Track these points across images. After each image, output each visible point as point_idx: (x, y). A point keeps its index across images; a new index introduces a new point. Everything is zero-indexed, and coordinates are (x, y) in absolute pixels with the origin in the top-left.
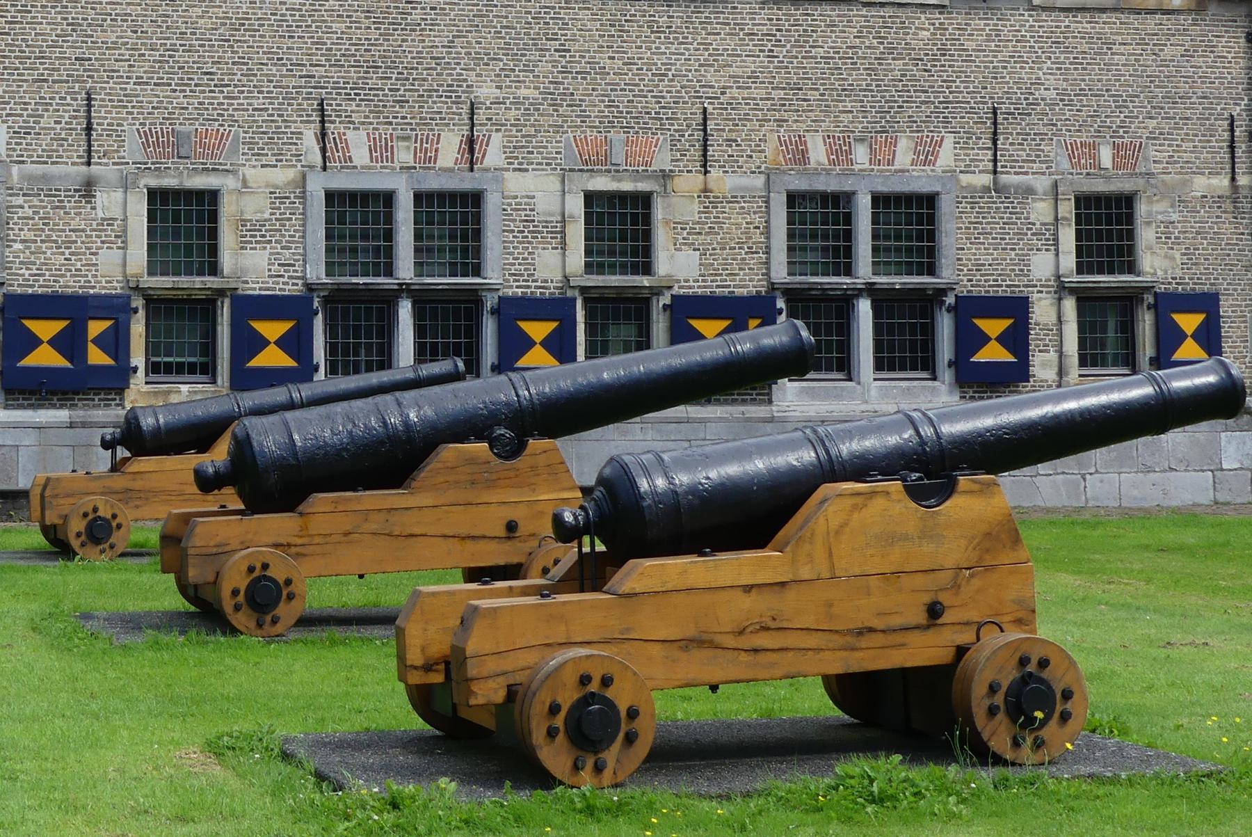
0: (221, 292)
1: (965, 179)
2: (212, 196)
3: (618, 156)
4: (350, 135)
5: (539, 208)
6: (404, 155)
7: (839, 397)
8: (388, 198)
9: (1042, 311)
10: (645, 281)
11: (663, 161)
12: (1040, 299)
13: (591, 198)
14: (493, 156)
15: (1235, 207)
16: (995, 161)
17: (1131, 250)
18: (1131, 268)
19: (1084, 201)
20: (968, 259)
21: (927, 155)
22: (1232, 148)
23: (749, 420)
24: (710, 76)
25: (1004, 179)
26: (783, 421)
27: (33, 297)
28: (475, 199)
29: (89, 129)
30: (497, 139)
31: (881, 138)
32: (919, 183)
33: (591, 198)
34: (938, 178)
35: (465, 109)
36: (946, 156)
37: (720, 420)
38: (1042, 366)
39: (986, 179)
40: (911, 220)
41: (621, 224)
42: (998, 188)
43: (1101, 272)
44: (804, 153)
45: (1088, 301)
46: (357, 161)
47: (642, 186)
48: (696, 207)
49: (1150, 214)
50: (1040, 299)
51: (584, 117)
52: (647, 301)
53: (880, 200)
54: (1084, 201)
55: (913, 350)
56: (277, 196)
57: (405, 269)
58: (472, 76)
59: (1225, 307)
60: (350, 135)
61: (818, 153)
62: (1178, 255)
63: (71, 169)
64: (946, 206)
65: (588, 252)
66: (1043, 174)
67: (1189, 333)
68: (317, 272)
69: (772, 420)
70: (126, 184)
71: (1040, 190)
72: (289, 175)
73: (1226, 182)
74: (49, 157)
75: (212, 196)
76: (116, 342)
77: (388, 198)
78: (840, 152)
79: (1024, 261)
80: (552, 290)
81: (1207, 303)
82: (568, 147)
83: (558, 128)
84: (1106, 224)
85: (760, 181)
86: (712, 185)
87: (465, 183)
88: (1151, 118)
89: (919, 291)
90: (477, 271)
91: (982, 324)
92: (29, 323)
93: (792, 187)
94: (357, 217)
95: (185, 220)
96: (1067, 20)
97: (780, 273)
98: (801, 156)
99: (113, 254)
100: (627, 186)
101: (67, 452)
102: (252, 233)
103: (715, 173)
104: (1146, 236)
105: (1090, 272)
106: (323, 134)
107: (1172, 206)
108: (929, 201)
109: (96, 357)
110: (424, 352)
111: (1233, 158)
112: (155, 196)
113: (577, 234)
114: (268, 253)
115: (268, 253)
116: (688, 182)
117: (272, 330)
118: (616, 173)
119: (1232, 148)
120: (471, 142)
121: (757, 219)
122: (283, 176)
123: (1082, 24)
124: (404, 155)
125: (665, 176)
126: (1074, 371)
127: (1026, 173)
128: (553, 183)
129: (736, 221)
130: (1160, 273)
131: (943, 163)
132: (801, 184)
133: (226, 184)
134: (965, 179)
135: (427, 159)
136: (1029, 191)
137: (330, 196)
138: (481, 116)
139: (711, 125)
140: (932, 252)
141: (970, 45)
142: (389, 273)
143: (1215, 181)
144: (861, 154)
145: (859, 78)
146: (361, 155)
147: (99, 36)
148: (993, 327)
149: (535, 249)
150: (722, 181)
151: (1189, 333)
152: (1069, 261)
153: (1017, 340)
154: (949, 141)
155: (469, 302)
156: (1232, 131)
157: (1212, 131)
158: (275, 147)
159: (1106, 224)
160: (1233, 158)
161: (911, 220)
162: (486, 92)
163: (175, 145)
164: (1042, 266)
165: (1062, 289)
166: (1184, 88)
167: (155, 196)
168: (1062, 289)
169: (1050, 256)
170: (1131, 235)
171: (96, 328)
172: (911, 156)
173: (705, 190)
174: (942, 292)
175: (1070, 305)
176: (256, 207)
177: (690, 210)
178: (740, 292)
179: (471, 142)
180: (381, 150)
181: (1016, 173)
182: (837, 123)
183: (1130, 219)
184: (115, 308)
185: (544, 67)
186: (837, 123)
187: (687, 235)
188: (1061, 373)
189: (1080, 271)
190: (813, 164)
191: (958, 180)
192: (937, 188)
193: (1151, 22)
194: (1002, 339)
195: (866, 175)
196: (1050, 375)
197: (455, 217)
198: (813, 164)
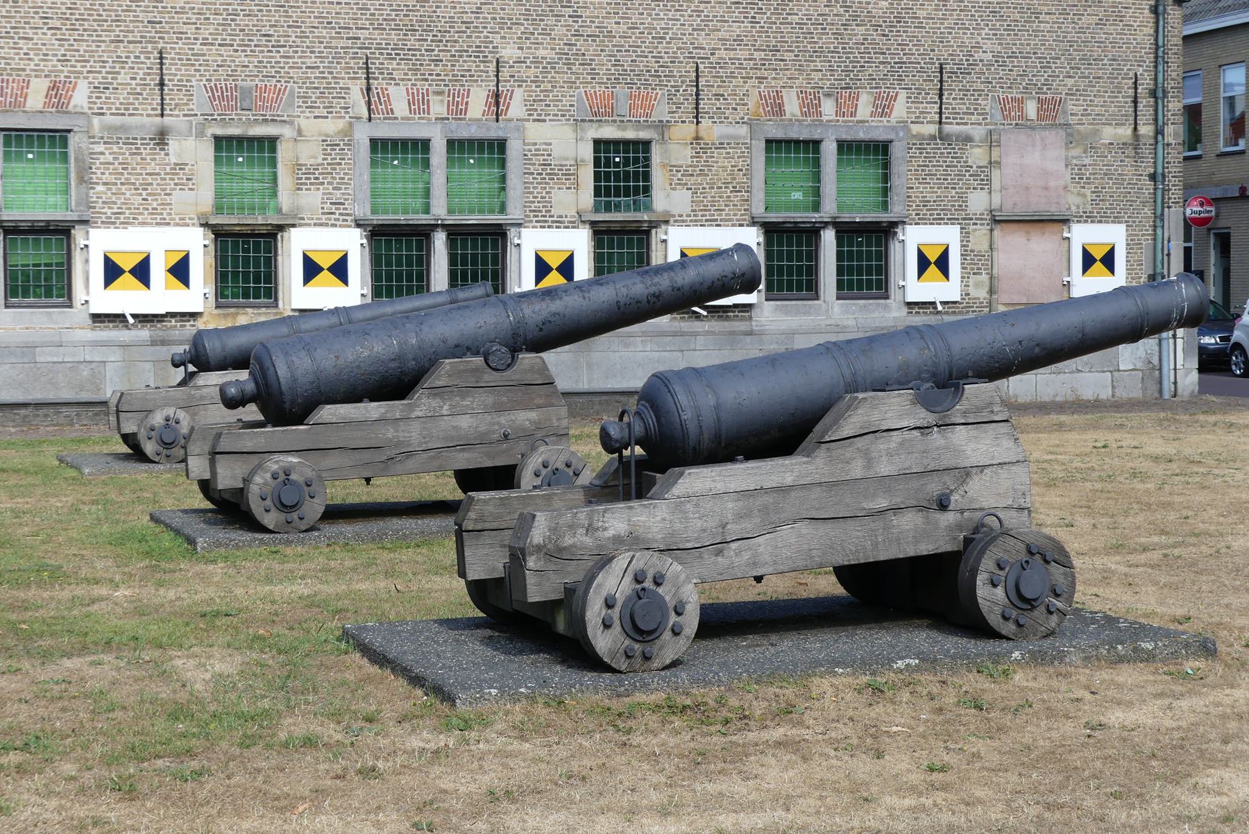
1: (915, 129)
4: (392, 90)
6: (438, 108)
11: (661, 112)
14: (516, 108)
16: (941, 113)
21: (883, 108)
22: (1135, 102)
24: (702, 39)
25: (947, 128)
26: (761, 333)
28: (500, 146)
30: (519, 94)
31: (846, 93)
33: (597, 143)
34: (893, 128)
35: (492, 67)
36: (900, 109)
37: (708, 333)
39: (932, 129)
42: (942, 136)
44: (781, 106)
47: (643, 135)
48: (689, 152)
51: (594, 74)
52: (648, 233)
53: (845, 147)
56: (329, 144)
58: (497, 39)
60: (392, 90)
61: (792, 106)
64: (897, 151)
65: (597, 192)
66: (980, 124)
69: (750, 333)
70: (201, 134)
71: (977, 138)
72: (341, 124)
78: (811, 106)
79: (962, 198)
82: (580, 100)
86: (701, 134)
90: (503, 209)
93: (770, 136)
98: (779, 109)
100: (630, 134)
103: (705, 123)
106: (369, 89)
110: (456, 278)
113: (587, 175)
118: (622, 125)
119: (1135, 102)
120: (497, 95)
122: (332, 126)
124: (438, 108)
125: (662, 127)
127: (966, 124)
132: (780, 135)
133: (287, 132)
134: (915, 129)
135: (458, 110)
136: (968, 139)
137: (374, 142)
138: (505, 73)
139: (702, 82)
142: (427, 211)
144: (828, 108)
145: (828, 42)
146: (400, 108)
150: (712, 130)
154: (903, 95)
156: (1136, 88)
157: (1119, 88)
158: (325, 99)
162: (509, 52)
163: (245, 99)
166: (1097, 52)
172: (871, 109)
173: (697, 138)
176: (310, 153)
177: (683, 155)
179: (497, 95)
180: (418, 104)
181: (958, 124)
185: (559, 31)
190: (788, 116)
191: (909, 130)
195: (830, 123)
198: (788, 116)
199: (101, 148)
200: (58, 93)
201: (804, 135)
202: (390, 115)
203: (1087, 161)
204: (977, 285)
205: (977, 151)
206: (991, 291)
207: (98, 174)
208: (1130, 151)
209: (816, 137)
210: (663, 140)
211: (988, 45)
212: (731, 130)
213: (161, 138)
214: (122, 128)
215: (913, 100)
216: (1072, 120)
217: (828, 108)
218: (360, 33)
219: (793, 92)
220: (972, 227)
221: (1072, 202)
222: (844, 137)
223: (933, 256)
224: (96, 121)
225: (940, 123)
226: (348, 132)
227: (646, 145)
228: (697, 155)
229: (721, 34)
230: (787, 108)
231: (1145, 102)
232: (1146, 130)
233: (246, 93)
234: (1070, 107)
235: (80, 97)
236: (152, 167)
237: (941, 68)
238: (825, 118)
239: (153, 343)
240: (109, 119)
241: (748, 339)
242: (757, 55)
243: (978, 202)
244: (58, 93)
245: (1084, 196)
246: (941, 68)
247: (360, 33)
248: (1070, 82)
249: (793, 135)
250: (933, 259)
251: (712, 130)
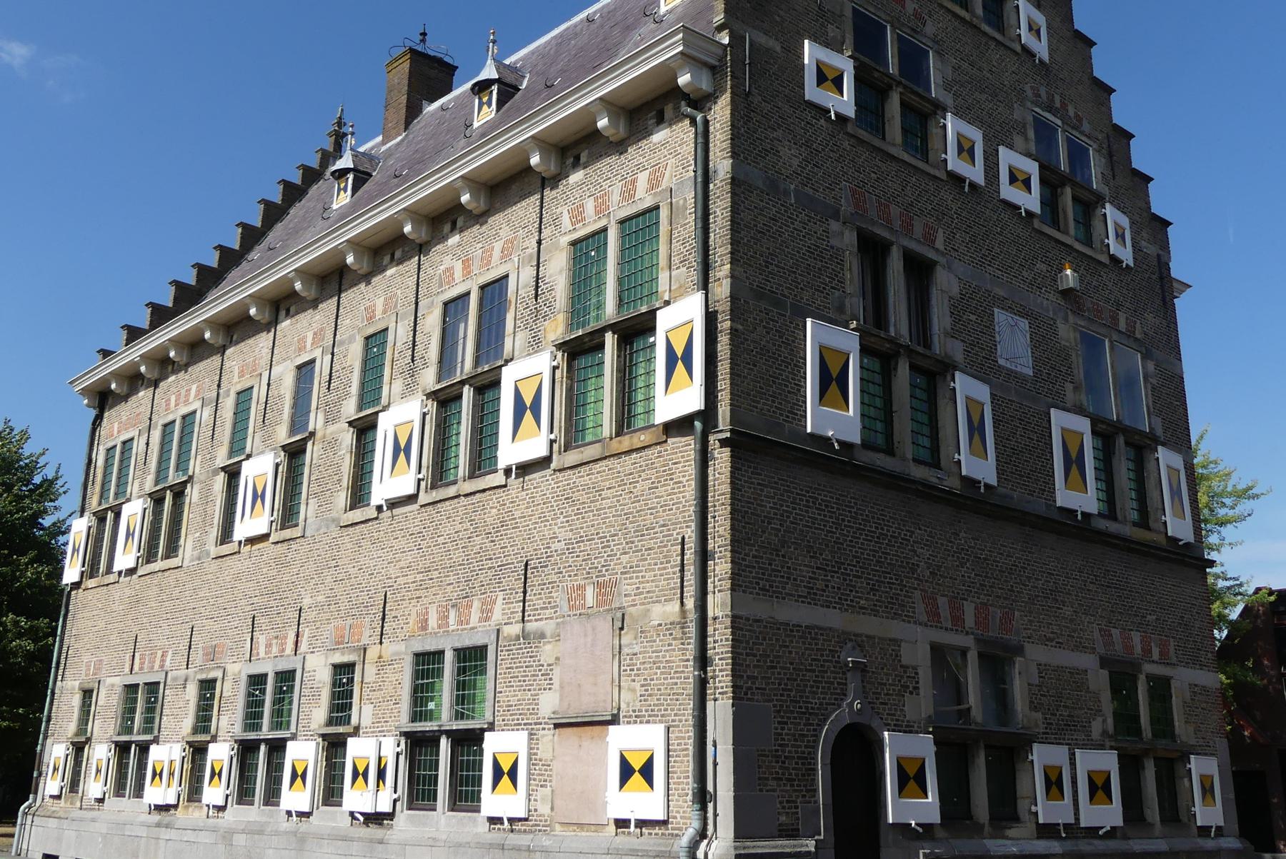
12: (543, 736)
15: (684, 633)
22: (682, 571)
25: (532, 626)
39: (515, 629)
50: (543, 736)
67: (637, 774)
71: (548, 634)
88: (625, 553)
119: (682, 571)
136: (542, 636)
141: (517, 514)
145: (458, 556)
151: (637, 774)
206: (552, 809)
209: (440, 647)
211: (562, 534)
216: (625, 602)
220: (541, 732)
221: (628, 700)
222: (459, 645)
223: (637, 764)
225: (523, 621)
229: (402, 564)
230: (430, 622)
234: (626, 588)
237: (526, 565)
238: (451, 628)
243: (549, 704)
246: (526, 565)
248: (625, 558)
250: (637, 766)
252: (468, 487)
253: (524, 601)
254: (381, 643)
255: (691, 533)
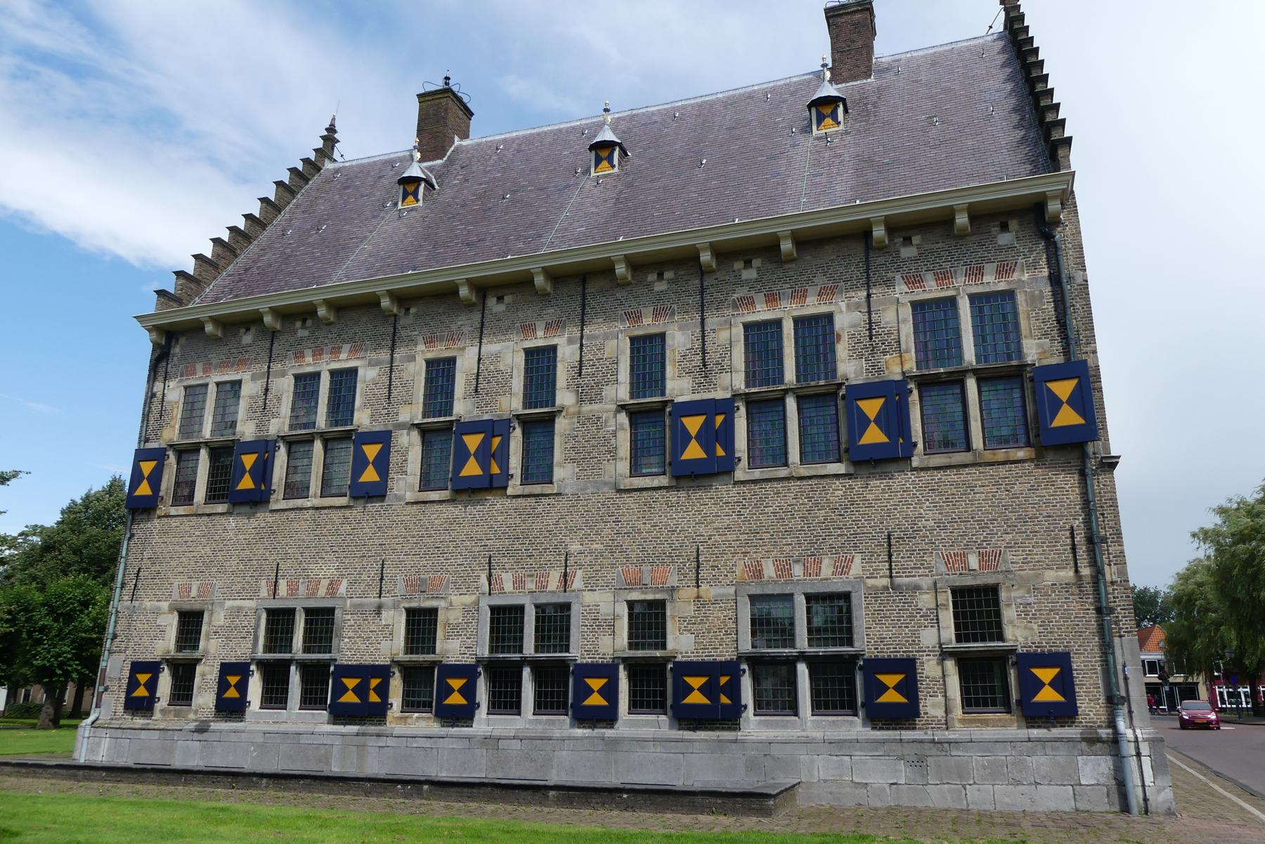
0: (434, 663)
1: (870, 582)
2: (433, 612)
3: (647, 580)
5: (602, 611)
7: (785, 727)
8: (520, 609)
9: (929, 668)
10: (658, 653)
11: (673, 581)
13: (631, 604)
14: (577, 583)
16: (890, 569)
17: (999, 625)
18: (1001, 637)
19: (958, 592)
20: (871, 636)
21: (843, 568)
23: (721, 741)
25: (898, 581)
26: (743, 742)
27: (351, 666)
28: (566, 607)
29: (382, 579)
30: (580, 573)
31: (811, 559)
32: (838, 585)
34: (849, 583)
36: (856, 568)
38: (931, 707)
40: (835, 610)
41: (648, 620)
43: (975, 640)
45: (966, 664)
46: (506, 590)
47: (659, 596)
48: (692, 608)
49: (1009, 598)
51: (628, 559)
54: (958, 592)
55: (842, 695)
56: (466, 610)
57: (529, 648)
59: (1077, 663)
61: (769, 570)
62: (1035, 627)
63: (372, 600)
65: (630, 637)
68: (485, 652)
70: (395, 607)
71: (925, 586)
72: (473, 598)
73: (1071, 573)
74: (364, 595)
75: (433, 612)
76: (383, 690)
77: (520, 609)
78: (784, 570)
80: (608, 660)
81: (1061, 660)
82: (619, 576)
83: (613, 565)
84: (977, 607)
85: (732, 590)
86: (702, 594)
87: (561, 599)
89: (838, 658)
91: (689, 680)
92: (880, 677)
94: (505, 620)
95: (422, 625)
96: (939, 475)
97: (746, 646)
98: (759, 573)
99: (386, 642)
100: (650, 597)
101: (354, 748)
102: (454, 630)
103: (704, 587)
104: (1009, 614)
105: (967, 641)
106: (490, 575)
107: (1028, 592)
108: (846, 596)
109: (374, 698)
111: (1075, 556)
112: (410, 612)
114: (461, 643)
115: (461, 643)
116: (689, 593)
117: (456, 683)
118: (644, 588)
121: (731, 614)
123: (952, 476)
124: (531, 586)
125: (673, 590)
126: (958, 712)
128: (609, 597)
129: (717, 615)
130: (1021, 639)
131: (858, 573)
132: (758, 591)
133: (441, 604)
134: (870, 582)
135: (543, 587)
136: (917, 588)
138: (571, 561)
139: (702, 559)
140: (850, 630)
143: (1062, 573)
144: (798, 570)
145: (796, 523)
146: (508, 586)
147: (390, 532)
148: (891, 680)
149: (600, 636)
150: (708, 591)
152: (949, 633)
153: (910, 687)
154: (858, 558)
155: (562, 666)
156: (1073, 537)
158: (465, 584)
159: (977, 607)
160: (1075, 556)
161: (835, 610)
162: (575, 547)
163: (420, 586)
164: (928, 638)
165: (944, 655)
167: (410, 612)
168: (944, 655)
169: (935, 630)
170: (998, 614)
171: (374, 682)
172: (832, 569)
173: (698, 597)
174: (856, 656)
175: (950, 665)
177: (690, 610)
178: (719, 659)
179: (565, 575)
180: (519, 583)
182: (782, 552)
183: (997, 602)
184: (383, 672)
186: (782, 552)
187: (688, 625)
188: (947, 711)
189: (959, 640)
190: (766, 578)
191: (865, 584)
192: (848, 589)
193: (1002, 470)
194: (461, 691)
196: (940, 713)
197: (555, 621)
198: (766, 578)
199: (349, 617)
200: (333, 586)
201: (778, 590)
202: (502, 592)
203: (1031, 600)
204: (934, 706)
205: (925, 597)
207: (347, 633)
208: (1075, 590)
210: (673, 600)
212: (722, 591)
213: (379, 610)
214: (361, 605)
215: (867, 561)
217: (798, 570)
218: (488, 543)
219: (770, 562)
224: (349, 601)
226: (477, 603)
227: (662, 604)
228: (698, 609)
231: (1082, 551)
232: (1086, 571)
233: (423, 581)
234: (1010, 557)
235: (343, 588)
236: (373, 627)
239: (357, 735)
240: (355, 600)
241: (734, 746)
242: (741, 537)
244: (333, 586)
245: (1032, 629)
247: (488, 543)
249: (769, 590)
251: (708, 591)
252: (804, 471)
253: (890, 561)
254: (698, 587)
255: (1078, 523)
